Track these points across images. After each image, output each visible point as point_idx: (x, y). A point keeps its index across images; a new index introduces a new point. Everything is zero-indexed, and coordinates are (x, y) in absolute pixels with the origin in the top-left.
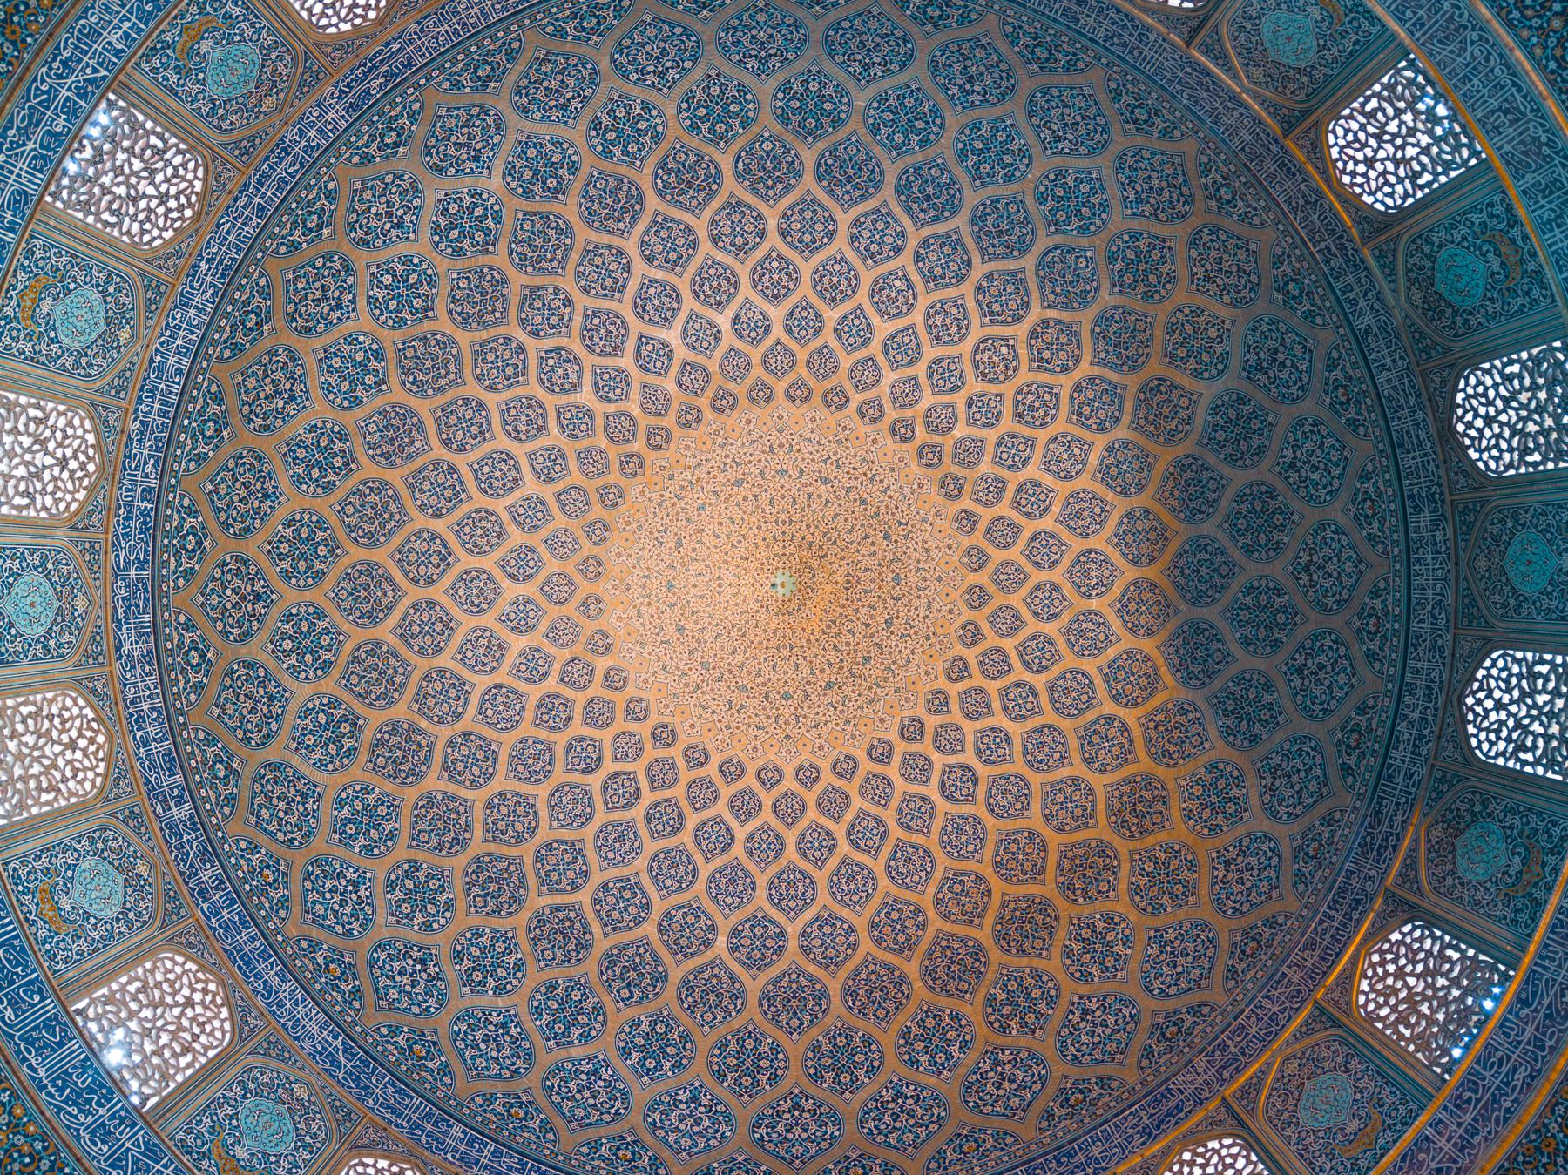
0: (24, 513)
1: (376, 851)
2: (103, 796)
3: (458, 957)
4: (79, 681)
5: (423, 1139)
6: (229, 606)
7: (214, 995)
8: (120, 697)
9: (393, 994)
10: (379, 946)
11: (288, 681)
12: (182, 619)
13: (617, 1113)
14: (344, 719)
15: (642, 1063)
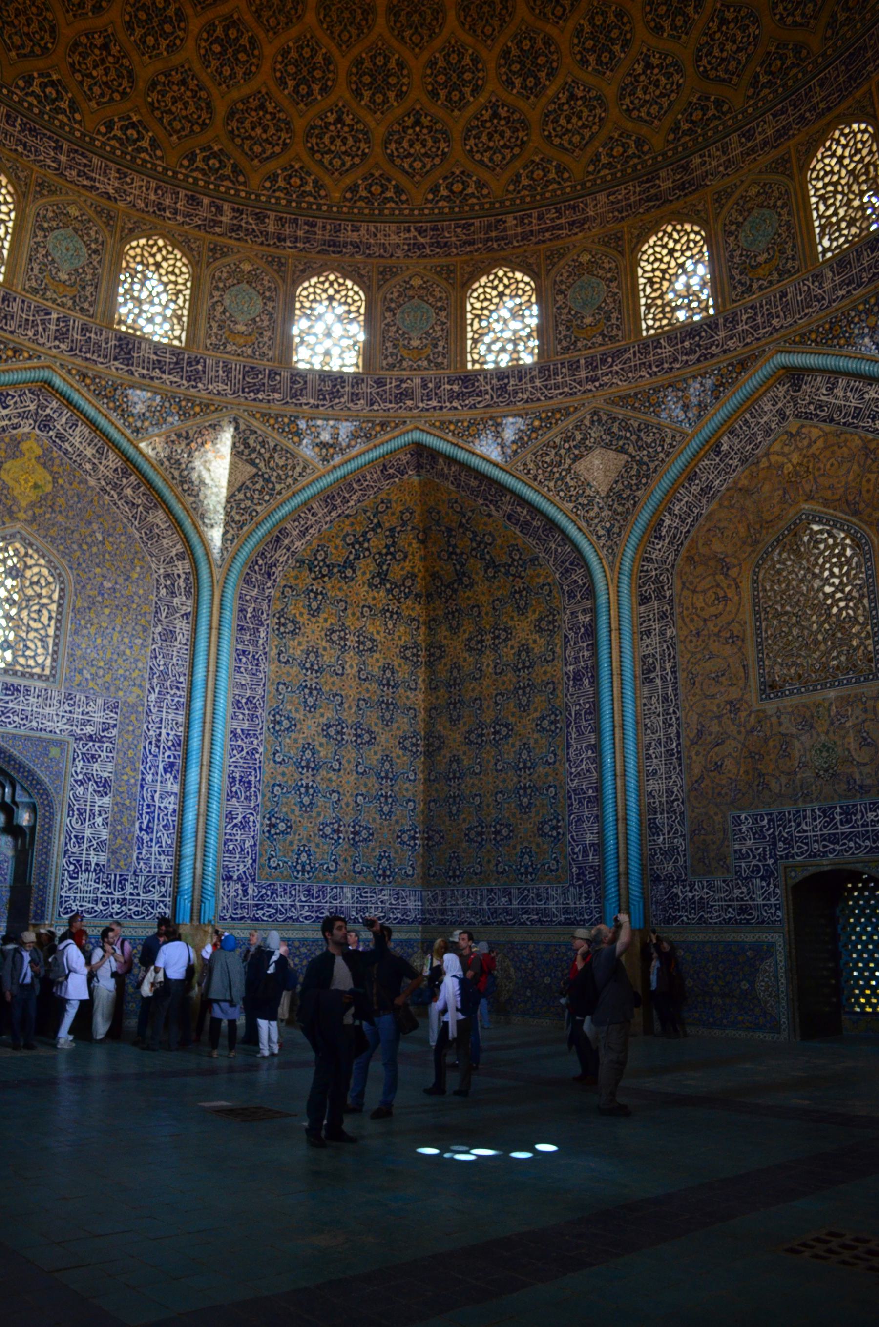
0: (10, 231)
1: (329, 83)
2: (194, 263)
3: (434, 94)
4: (122, 239)
5: (495, 246)
6: (104, 79)
7: (336, 280)
8: (140, 214)
9: (418, 165)
10: (387, 142)
11: (176, 59)
12: (103, 129)
13: (601, 119)
14: (226, 29)
15: (599, 62)
